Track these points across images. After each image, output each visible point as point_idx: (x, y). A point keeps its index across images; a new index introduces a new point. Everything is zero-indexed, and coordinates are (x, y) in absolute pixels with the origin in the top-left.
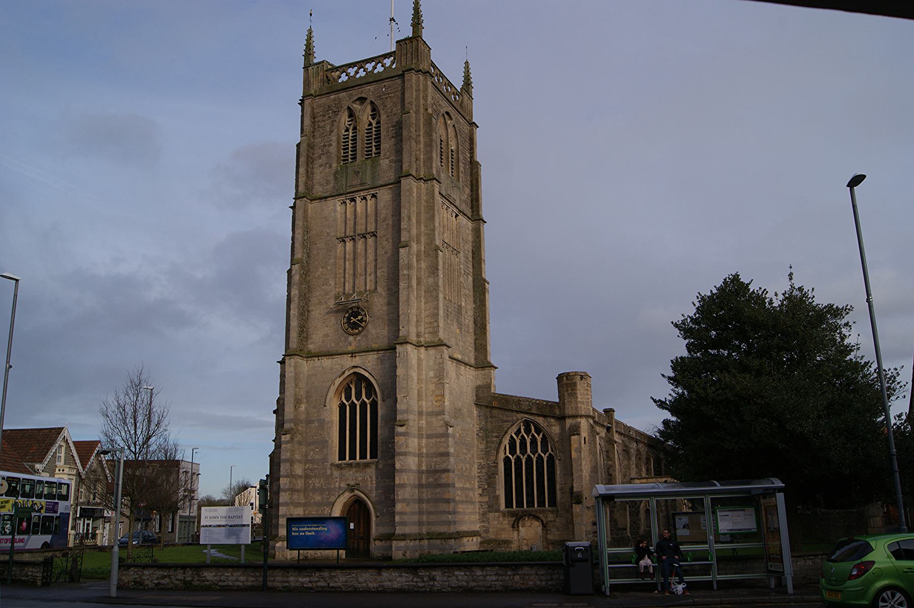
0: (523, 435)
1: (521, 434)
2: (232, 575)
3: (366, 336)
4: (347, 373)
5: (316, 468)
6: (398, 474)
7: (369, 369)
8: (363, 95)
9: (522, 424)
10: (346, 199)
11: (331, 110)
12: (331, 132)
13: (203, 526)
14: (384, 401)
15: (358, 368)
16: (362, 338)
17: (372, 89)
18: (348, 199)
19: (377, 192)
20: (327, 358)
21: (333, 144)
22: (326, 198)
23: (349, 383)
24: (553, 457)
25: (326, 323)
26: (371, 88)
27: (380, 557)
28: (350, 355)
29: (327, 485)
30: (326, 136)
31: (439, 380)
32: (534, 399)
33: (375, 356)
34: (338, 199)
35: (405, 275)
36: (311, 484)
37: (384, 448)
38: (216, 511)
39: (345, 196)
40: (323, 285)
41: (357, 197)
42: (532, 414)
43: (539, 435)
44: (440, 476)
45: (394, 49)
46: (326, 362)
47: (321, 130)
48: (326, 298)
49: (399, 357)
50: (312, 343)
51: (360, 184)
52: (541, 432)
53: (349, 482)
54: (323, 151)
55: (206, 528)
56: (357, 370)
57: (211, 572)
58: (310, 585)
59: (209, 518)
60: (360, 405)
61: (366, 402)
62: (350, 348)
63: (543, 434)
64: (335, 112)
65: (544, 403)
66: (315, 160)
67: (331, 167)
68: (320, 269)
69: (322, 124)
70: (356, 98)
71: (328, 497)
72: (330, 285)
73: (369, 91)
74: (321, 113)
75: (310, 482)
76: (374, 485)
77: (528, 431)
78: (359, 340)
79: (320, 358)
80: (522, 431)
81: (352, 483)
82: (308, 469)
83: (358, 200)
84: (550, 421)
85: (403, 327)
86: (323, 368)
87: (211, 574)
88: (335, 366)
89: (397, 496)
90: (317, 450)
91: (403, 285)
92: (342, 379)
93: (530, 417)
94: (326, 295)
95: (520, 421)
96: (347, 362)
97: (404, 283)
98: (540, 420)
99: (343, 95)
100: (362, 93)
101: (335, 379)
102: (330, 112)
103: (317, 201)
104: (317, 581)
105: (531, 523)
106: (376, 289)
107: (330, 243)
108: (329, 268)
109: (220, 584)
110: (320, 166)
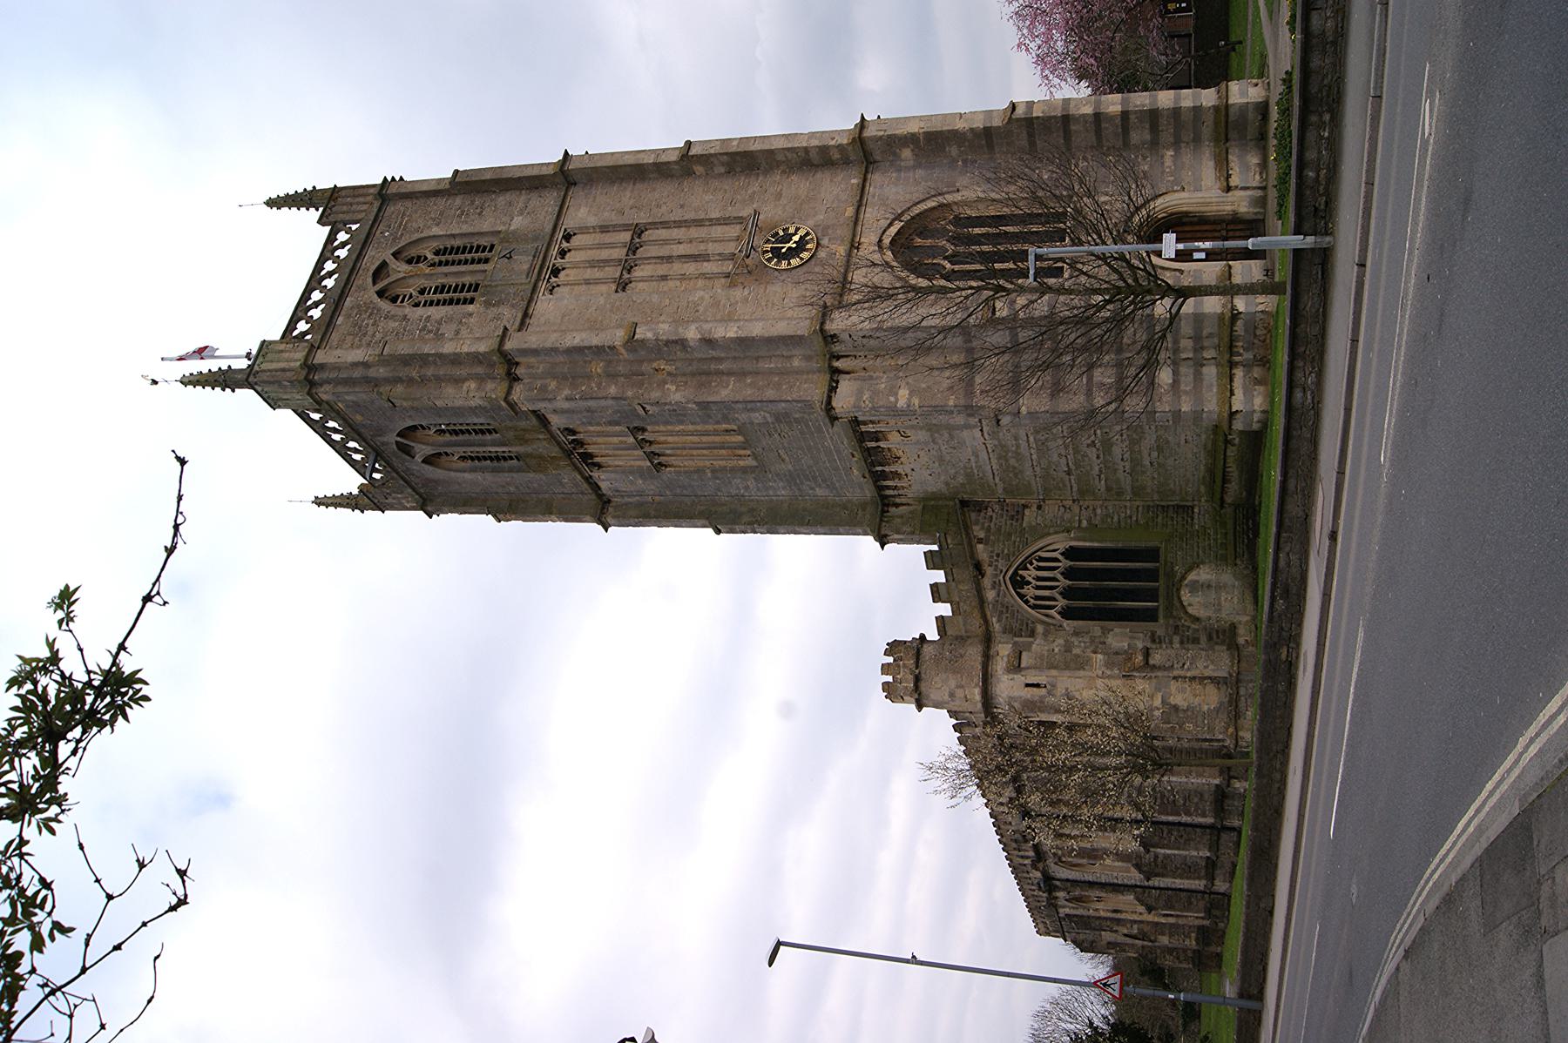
12: (405, 317)
18: (550, 278)
19: (563, 230)
21: (429, 313)
34: (541, 294)
40: (697, 311)
48: (724, 306)
49: (885, 131)
54: (430, 332)
56: (887, 241)
64: (371, 314)
72: (702, 298)
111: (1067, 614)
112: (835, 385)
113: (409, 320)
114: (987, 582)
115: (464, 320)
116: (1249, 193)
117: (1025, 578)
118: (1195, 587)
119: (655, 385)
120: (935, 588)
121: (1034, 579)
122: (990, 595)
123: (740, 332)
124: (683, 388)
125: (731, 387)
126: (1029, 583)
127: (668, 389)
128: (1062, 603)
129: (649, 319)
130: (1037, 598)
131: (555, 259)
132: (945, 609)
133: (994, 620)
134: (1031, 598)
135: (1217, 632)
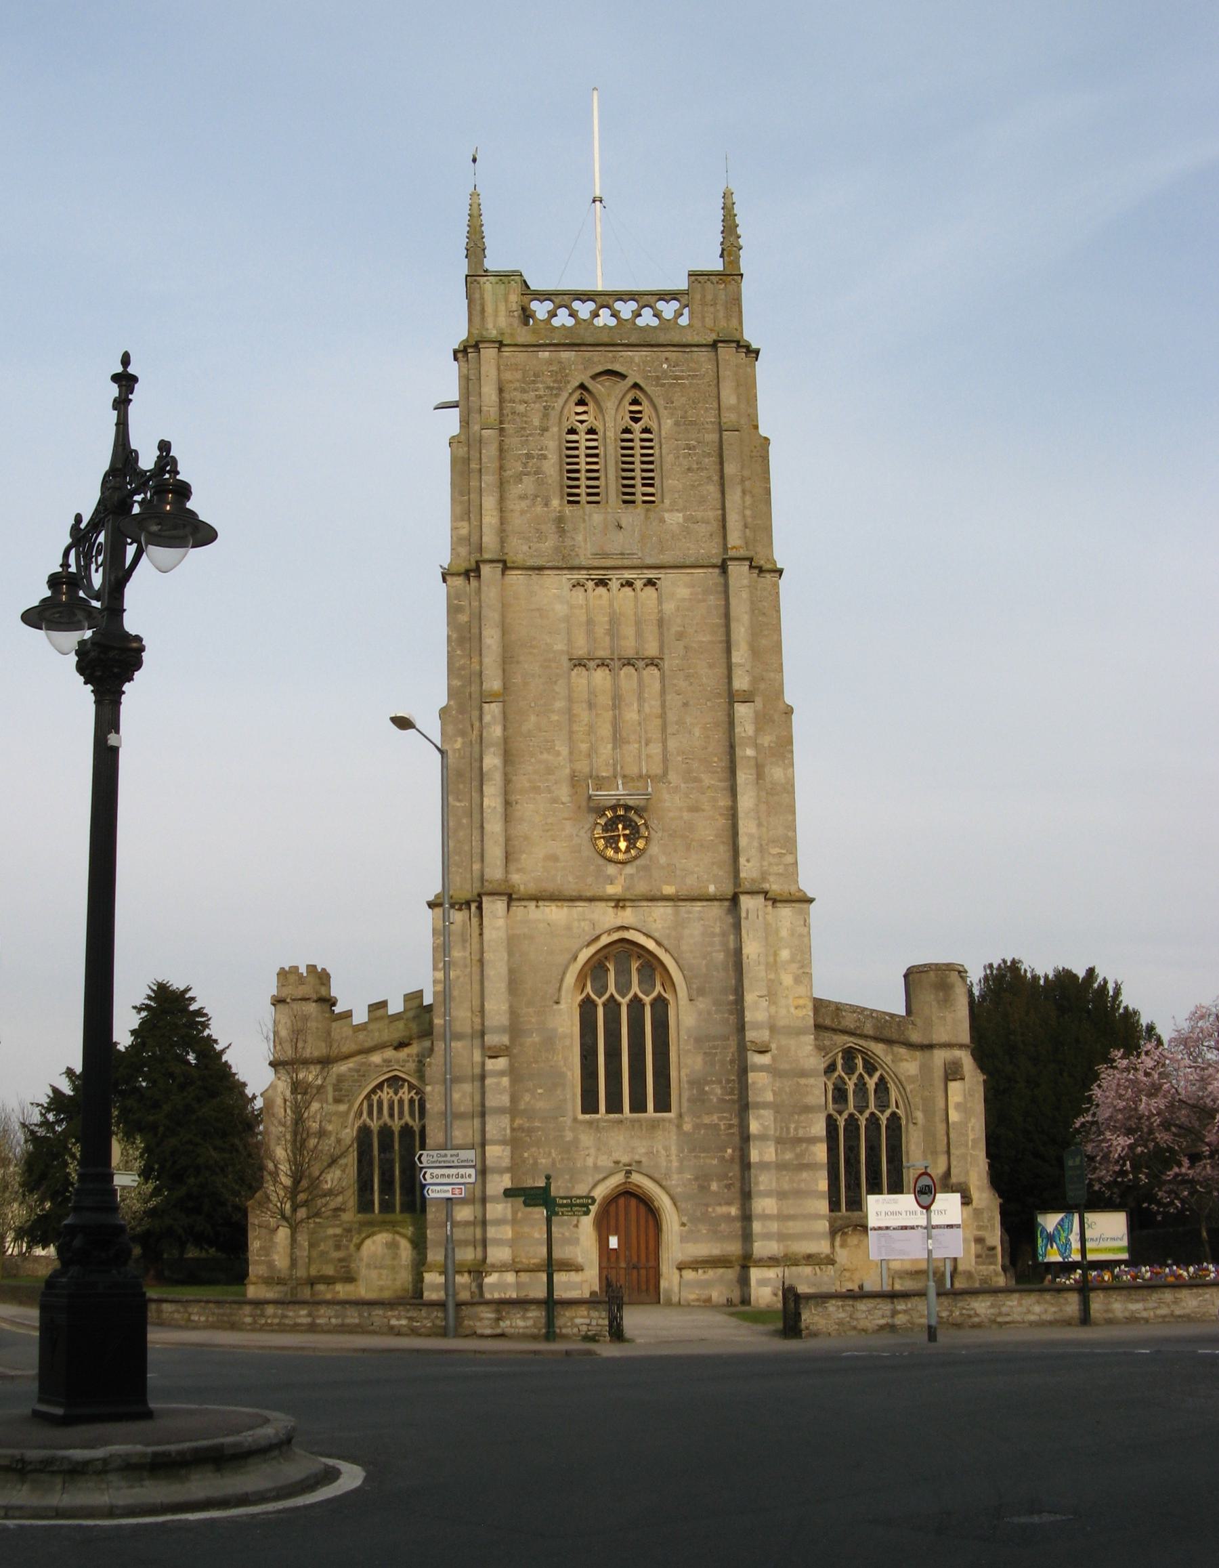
0: (861, 1075)
1: (836, 1074)
2: (1021, 1305)
3: (646, 868)
4: (605, 940)
5: (539, 1127)
6: (757, 1143)
7: (656, 935)
8: (617, 367)
9: (840, 1054)
10: (587, 579)
11: (542, 382)
12: (545, 429)
13: (874, 1229)
14: (691, 1000)
15: (631, 931)
16: (638, 872)
17: (637, 360)
19: (659, 576)
20: (559, 904)
21: (550, 456)
22: (540, 569)
23: (603, 959)
24: (899, 1118)
25: (550, 833)
26: (638, 356)
27: (693, 1301)
28: (613, 904)
29: (565, 1162)
30: (530, 435)
31: (802, 967)
32: (865, 1009)
33: (669, 910)
35: (749, 757)
36: (528, 1158)
37: (695, 1091)
38: (896, 1202)
39: (585, 572)
40: (541, 753)
41: (614, 580)
42: (866, 1037)
43: (871, 1076)
44: (807, 1149)
45: (684, 286)
46: (554, 913)
47: (518, 420)
49: (747, 918)
50: (519, 870)
51: (621, 554)
52: (875, 1069)
53: (617, 1156)
54: (525, 465)
55: (880, 1232)
57: (982, 1301)
58: (1145, 1314)
59: (883, 1214)
60: (628, 1006)
61: (641, 1000)
62: (611, 890)
63: (881, 1075)
64: (551, 388)
65: (887, 1018)
66: (509, 482)
67: (546, 505)
68: (533, 718)
69: (521, 408)
70: (600, 369)
71: (569, 1185)
72: (558, 754)
73: (633, 363)
74: (518, 384)
75: (526, 1155)
76: (675, 1164)
77: (850, 1068)
78: (632, 876)
79: (540, 903)
80: (839, 1067)
81: (625, 1159)
82: (519, 1129)
83: (614, 585)
84: (898, 1053)
85: (748, 861)
86: (549, 924)
87: (983, 1305)
88: (576, 924)
89: (757, 1184)
90: (540, 1091)
91: (743, 776)
92: (592, 950)
93: (861, 1042)
94: (549, 774)
95: (840, 1049)
96: (607, 917)
97: (745, 774)
98: (878, 1049)
99: (566, 355)
100: (613, 361)
101: (581, 949)
102: (541, 386)
103: (520, 572)
104: (1156, 1308)
105: (860, 1240)
106: (665, 774)
107: (553, 665)
108: (555, 718)
109: (999, 1319)
110: (523, 497)
111: (364, 1132)
112: (457, 907)
113: (542, 435)
114: (390, 1053)
115: (539, 499)
116: (676, 1289)
117: (402, 1088)
118: (393, 1246)
119: (461, 727)
120: (383, 1004)
121: (401, 1097)
122: (376, 1058)
123: (489, 811)
124: (457, 755)
125: (458, 804)
126: (396, 1093)
127: (456, 741)
128: (375, 1125)
129: (533, 705)
130: (380, 1103)
131: (617, 579)
132: (360, 1016)
133: (351, 1065)
134: (380, 1097)
135: (347, 1267)
